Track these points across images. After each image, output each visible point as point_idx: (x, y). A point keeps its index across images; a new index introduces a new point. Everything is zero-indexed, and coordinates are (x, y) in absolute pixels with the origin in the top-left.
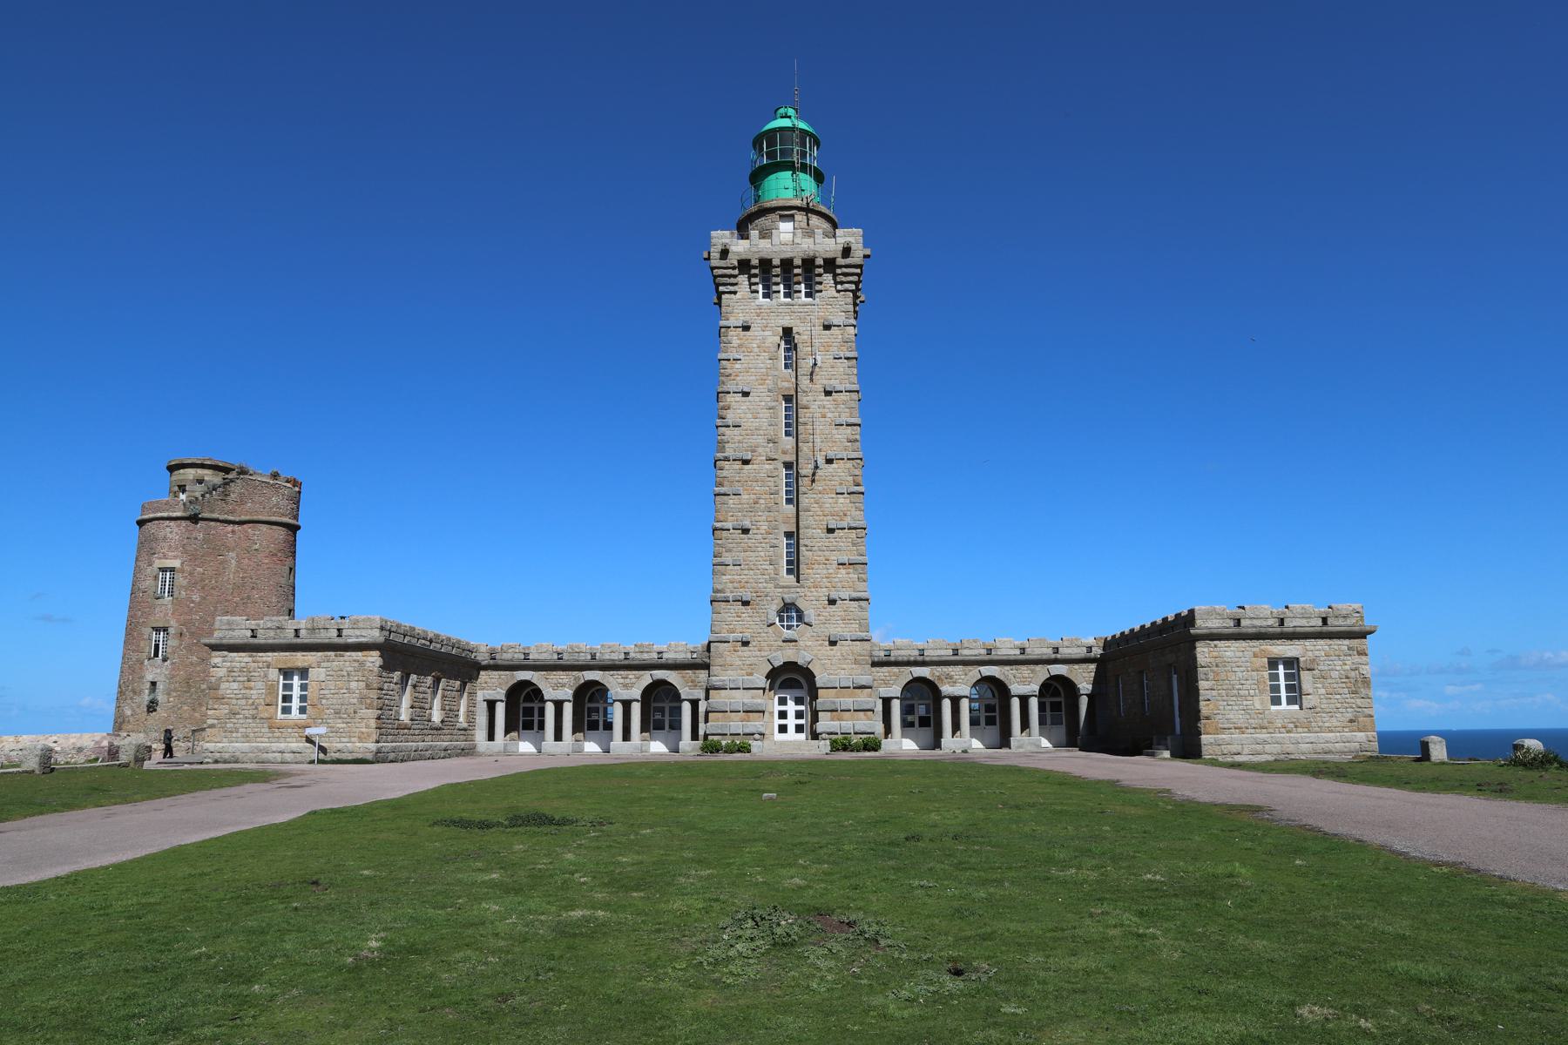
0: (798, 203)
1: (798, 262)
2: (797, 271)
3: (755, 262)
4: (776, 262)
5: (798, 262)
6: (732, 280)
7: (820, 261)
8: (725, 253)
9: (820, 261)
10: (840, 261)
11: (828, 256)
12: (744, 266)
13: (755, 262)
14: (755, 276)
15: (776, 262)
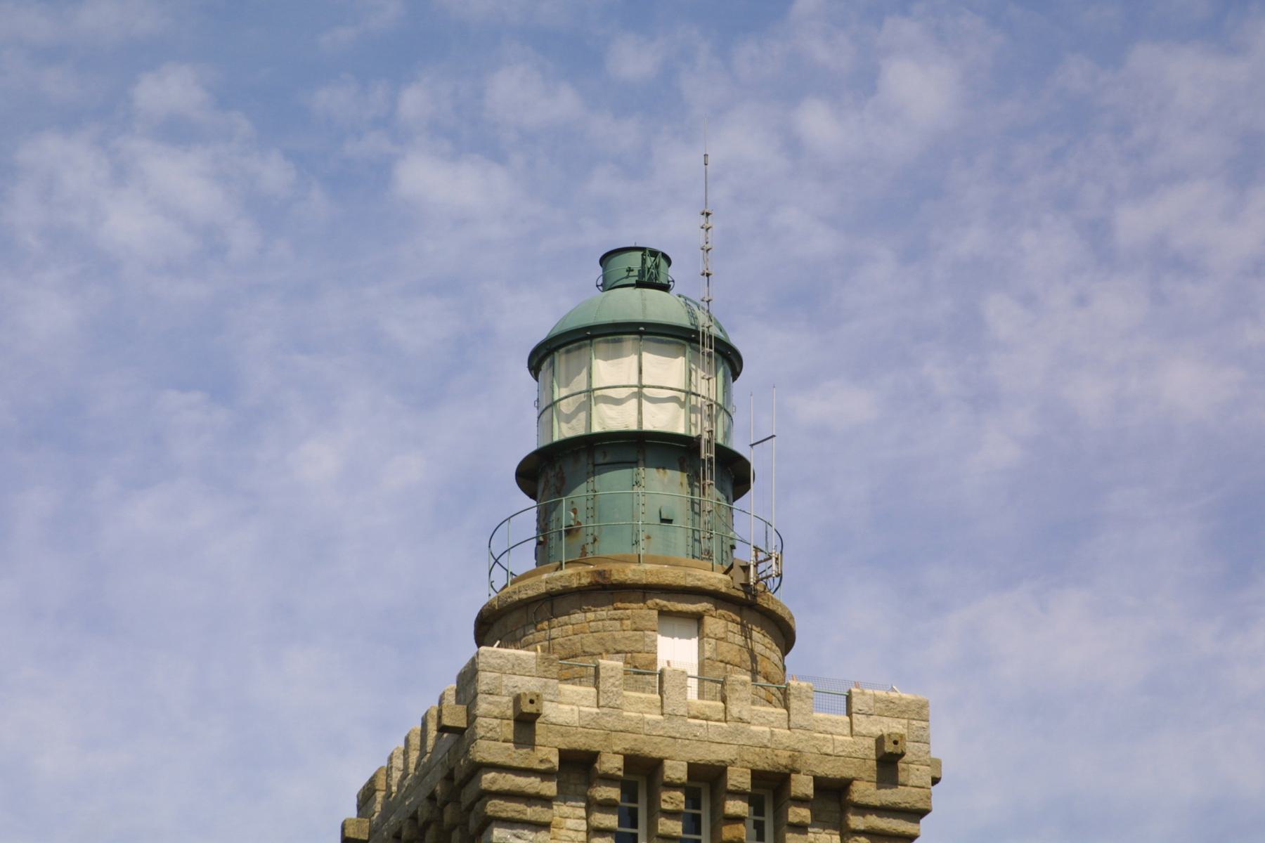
0: (714, 578)
1: (739, 778)
2: (735, 807)
3: (611, 763)
4: (676, 771)
5: (739, 778)
6: (533, 812)
7: (802, 785)
8: (526, 723)
9: (802, 785)
10: (865, 791)
11: (830, 770)
12: (577, 767)
13: (611, 763)
14: (607, 806)
15: (676, 771)
